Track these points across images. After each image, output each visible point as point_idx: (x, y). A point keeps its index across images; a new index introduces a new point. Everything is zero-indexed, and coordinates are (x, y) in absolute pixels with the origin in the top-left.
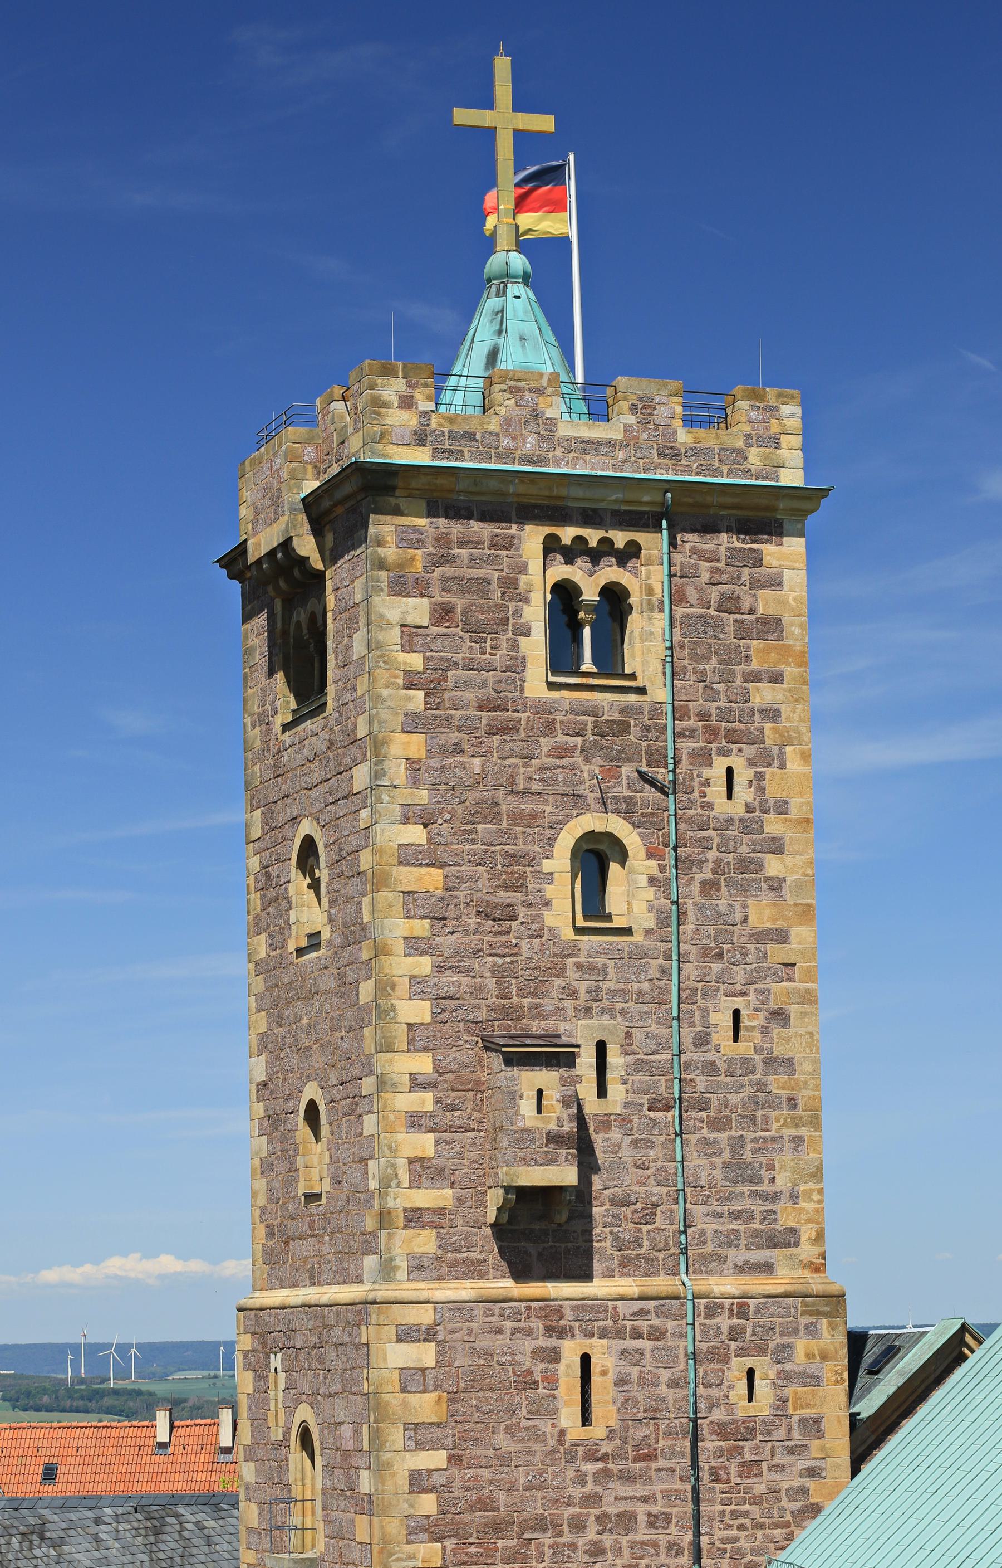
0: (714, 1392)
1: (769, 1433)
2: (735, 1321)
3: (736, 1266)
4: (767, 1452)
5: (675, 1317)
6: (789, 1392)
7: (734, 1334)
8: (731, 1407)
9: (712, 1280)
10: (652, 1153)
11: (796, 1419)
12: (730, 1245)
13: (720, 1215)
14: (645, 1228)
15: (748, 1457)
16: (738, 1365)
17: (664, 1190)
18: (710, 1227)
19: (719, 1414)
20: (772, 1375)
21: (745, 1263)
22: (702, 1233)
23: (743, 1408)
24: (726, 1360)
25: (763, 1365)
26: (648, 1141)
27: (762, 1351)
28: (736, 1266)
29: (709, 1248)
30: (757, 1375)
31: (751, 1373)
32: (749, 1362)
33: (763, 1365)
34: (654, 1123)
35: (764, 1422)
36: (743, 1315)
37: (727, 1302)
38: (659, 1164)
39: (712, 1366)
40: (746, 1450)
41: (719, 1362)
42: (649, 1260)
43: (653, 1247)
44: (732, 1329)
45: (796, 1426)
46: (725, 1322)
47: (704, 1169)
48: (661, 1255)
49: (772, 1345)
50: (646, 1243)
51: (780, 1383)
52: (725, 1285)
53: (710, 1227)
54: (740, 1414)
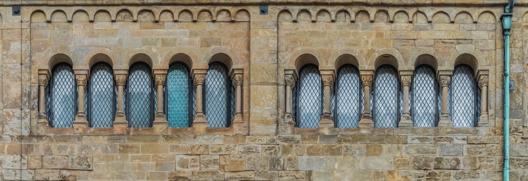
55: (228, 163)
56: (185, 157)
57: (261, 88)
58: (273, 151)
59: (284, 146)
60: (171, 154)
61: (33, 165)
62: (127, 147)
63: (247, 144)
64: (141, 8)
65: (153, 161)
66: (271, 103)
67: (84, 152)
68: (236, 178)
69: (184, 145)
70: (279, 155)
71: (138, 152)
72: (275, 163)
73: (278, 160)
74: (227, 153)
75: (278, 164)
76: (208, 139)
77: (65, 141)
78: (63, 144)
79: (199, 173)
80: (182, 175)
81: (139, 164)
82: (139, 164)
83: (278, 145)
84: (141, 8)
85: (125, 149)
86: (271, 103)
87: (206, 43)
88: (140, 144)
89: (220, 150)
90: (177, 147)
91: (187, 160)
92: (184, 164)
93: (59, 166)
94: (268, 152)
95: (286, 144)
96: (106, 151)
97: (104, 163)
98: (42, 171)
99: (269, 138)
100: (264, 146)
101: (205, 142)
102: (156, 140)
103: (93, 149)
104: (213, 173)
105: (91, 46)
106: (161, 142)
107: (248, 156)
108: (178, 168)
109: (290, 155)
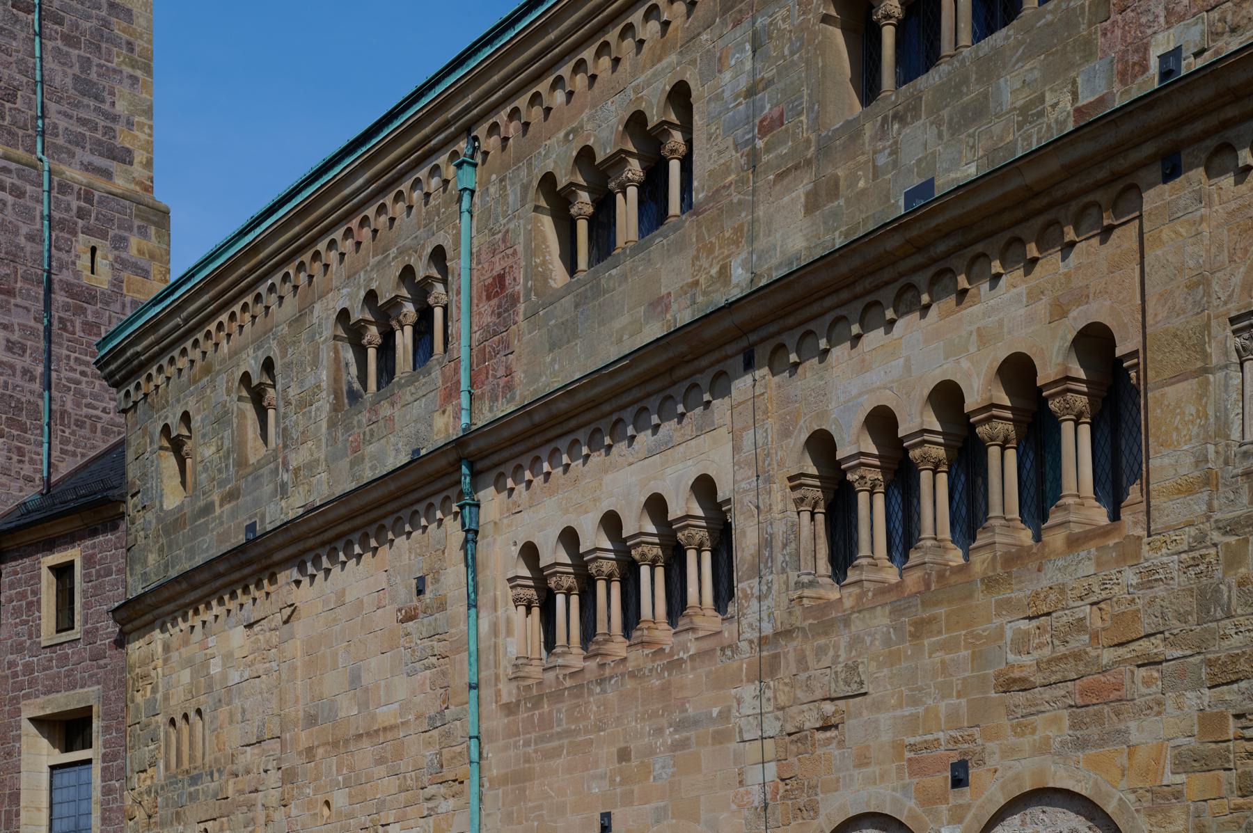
0: (63, 255)
1: (107, 304)
2: (82, 204)
3: (82, 163)
4: (106, 318)
5: (33, 183)
6: (125, 275)
7: (81, 214)
8: (77, 274)
9: (63, 167)
10: (14, 44)
11: (128, 300)
12: (78, 145)
13: (71, 117)
14: (8, 105)
15: (90, 318)
16: (82, 243)
17: (25, 80)
18: (63, 124)
19: (66, 275)
20: (111, 258)
21: (90, 164)
22: (55, 126)
23: (86, 278)
24: (75, 234)
25: (103, 246)
26: (12, 32)
27: (103, 235)
28: (82, 163)
29: (60, 141)
30: (98, 253)
31: (94, 250)
32: (94, 241)
33: (103, 246)
34: (17, 20)
35: (103, 293)
36: (88, 199)
37: (76, 187)
38: (20, 55)
39: (61, 234)
40: (89, 312)
41: (69, 233)
42: (9, 133)
43: (14, 123)
44: (80, 209)
45: (128, 305)
46: (75, 204)
47: (62, 77)
48: (21, 133)
49: (111, 233)
50: (8, 118)
51: (117, 266)
52: (74, 174)
53: (63, 124)
54: (85, 281)
55: (1108, 624)
56: (1024, 625)
57: (1172, 392)
58: (1202, 567)
59: (1228, 545)
60: (997, 621)
61: (782, 699)
62: (922, 620)
63: (1147, 560)
64: (932, 270)
65: (966, 648)
66: (1195, 430)
67: (854, 653)
68: (1125, 660)
69: (1021, 595)
70: (1219, 574)
71: (940, 633)
72: (1207, 600)
73: (1217, 590)
74: (1104, 595)
75: (1217, 602)
76: (1066, 567)
77: (826, 633)
78: (822, 641)
79: (1049, 662)
80: (1016, 674)
81: (943, 662)
82: (943, 662)
83: (1215, 545)
84: (932, 270)
85: (921, 628)
86: (1195, 430)
87: (1059, 311)
88: (942, 611)
89: (1090, 591)
90: (1008, 601)
91: (1027, 633)
92: (1022, 644)
93: (818, 694)
94: (1192, 572)
95: (1232, 539)
96: (887, 642)
97: (885, 671)
98: (795, 709)
99: (1192, 531)
100: (1184, 556)
101: (1059, 578)
102: (970, 596)
103: (868, 640)
104: (1077, 656)
105: (860, 395)
106: (980, 597)
107: (1150, 593)
108: (1011, 657)
109: (1243, 570)
